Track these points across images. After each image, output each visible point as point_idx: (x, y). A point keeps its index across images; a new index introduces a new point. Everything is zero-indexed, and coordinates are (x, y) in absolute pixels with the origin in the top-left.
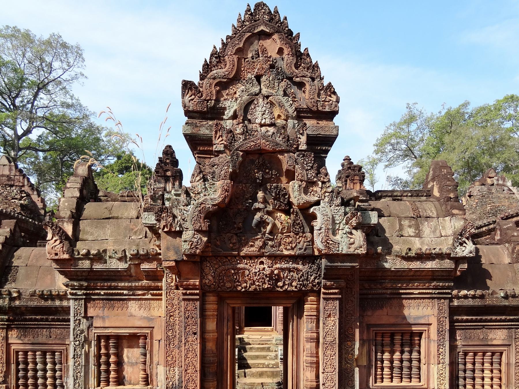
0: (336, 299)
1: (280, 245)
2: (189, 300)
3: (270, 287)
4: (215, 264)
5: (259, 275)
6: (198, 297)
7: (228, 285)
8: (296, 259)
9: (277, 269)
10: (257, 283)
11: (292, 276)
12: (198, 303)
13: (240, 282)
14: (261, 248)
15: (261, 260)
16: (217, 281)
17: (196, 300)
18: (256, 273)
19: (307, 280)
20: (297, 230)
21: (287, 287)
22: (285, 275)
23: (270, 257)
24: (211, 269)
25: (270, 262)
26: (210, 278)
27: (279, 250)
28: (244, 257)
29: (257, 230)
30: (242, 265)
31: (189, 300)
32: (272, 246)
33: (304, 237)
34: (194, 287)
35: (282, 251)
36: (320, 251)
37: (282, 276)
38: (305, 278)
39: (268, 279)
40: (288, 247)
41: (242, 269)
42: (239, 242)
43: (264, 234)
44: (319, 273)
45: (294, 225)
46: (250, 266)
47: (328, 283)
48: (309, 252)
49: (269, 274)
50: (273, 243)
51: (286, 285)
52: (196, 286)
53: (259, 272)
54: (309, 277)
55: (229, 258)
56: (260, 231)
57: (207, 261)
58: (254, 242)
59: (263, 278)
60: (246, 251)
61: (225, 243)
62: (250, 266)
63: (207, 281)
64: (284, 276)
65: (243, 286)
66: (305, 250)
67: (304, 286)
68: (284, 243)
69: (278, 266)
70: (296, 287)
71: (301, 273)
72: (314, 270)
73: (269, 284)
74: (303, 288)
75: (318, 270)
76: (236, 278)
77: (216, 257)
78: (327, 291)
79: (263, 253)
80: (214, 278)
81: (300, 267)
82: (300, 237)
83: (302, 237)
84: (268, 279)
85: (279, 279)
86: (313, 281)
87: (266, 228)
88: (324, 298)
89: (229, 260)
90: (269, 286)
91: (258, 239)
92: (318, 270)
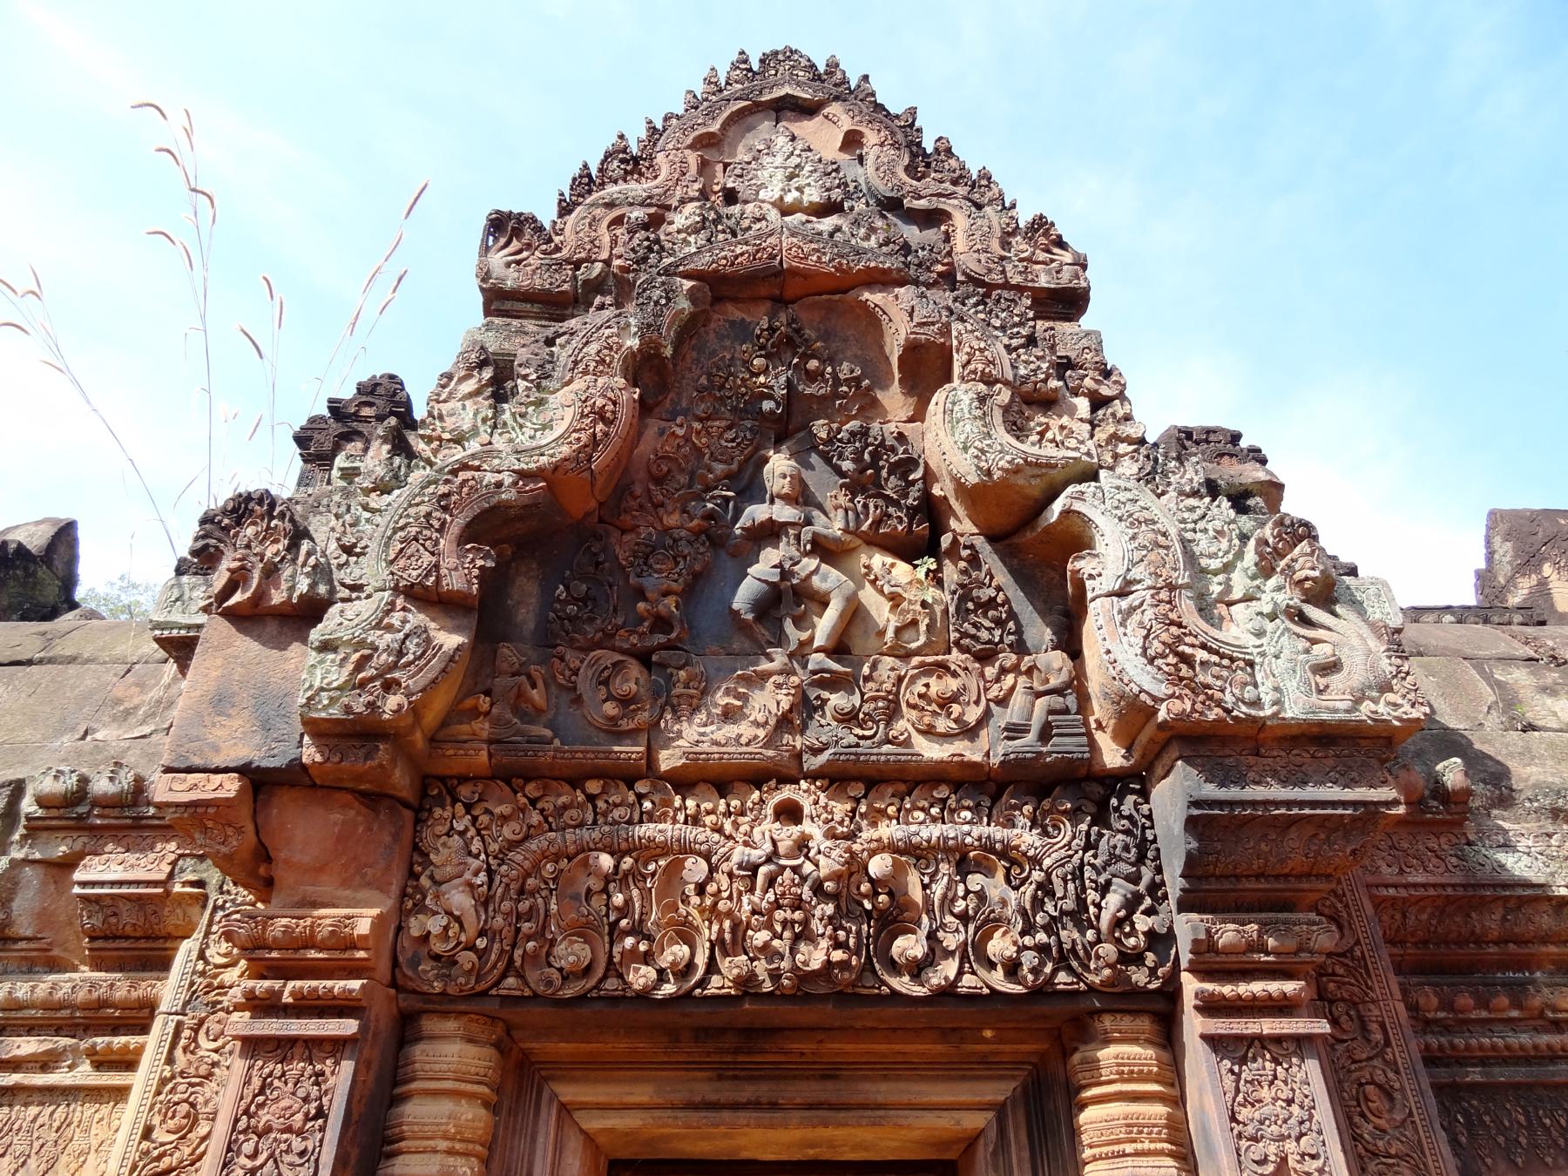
0: (1301, 1044)
1: (892, 712)
2: (282, 1048)
3: (844, 965)
4: (505, 818)
5: (771, 882)
6: (349, 1026)
7: (570, 953)
8: (995, 799)
9: (881, 847)
10: (762, 937)
11: (981, 896)
12: (341, 1076)
13: (649, 938)
14: (784, 723)
15: (787, 792)
16: (499, 921)
17: (336, 1047)
18: (754, 868)
19: (1079, 916)
20: (984, 635)
21: (949, 968)
22: (938, 889)
23: (835, 779)
24: (476, 845)
25: (840, 808)
26: (459, 899)
27: (889, 742)
28: (684, 782)
29: (763, 632)
30: (667, 826)
31: (282, 1048)
32: (849, 718)
33: (1029, 672)
34: (340, 954)
35: (907, 743)
36: (1134, 713)
37: (917, 894)
38: (1069, 904)
39: (829, 909)
40: (942, 724)
41: (664, 849)
42: (656, 695)
43: (800, 654)
44: (1147, 874)
45: (962, 612)
46: (719, 830)
47: (1228, 934)
48: (1065, 745)
49: (836, 877)
50: (856, 700)
51: (949, 954)
52: (352, 944)
53: (769, 860)
54: (1092, 896)
55: (593, 787)
56: (780, 640)
57: (455, 800)
58: (744, 698)
59: (798, 904)
60: (693, 737)
61: (578, 700)
62: (719, 830)
63: (435, 924)
64: (928, 900)
65: (665, 960)
66: (1045, 734)
67: (1063, 959)
68: (915, 700)
69: (889, 830)
70: (1012, 969)
71: (1037, 876)
72: (1113, 858)
73: (837, 945)
74: (1062, 977)
75: (1141, 859)
76: (625, 910)
77: (511, 775)
78: (1227, 990)
79: (798, 756)
80: (485, 902)
81: (1026, 838)
82: (1004, 671)
83: (1015, 669)
84: (829, 909)
85: (895, 919)
86: (1118, 923)
87: (813, 627)
88: (1214, 1042)
89: (591, 798)
90: (838, 955)
91: (764, 676)
92: (1141, 859)
